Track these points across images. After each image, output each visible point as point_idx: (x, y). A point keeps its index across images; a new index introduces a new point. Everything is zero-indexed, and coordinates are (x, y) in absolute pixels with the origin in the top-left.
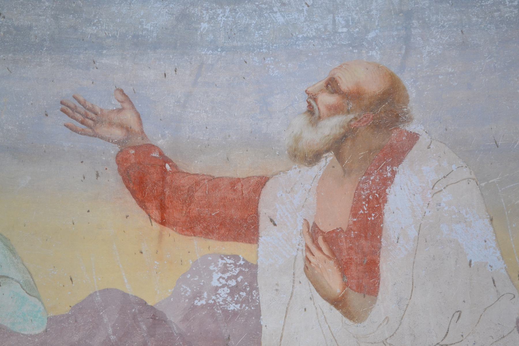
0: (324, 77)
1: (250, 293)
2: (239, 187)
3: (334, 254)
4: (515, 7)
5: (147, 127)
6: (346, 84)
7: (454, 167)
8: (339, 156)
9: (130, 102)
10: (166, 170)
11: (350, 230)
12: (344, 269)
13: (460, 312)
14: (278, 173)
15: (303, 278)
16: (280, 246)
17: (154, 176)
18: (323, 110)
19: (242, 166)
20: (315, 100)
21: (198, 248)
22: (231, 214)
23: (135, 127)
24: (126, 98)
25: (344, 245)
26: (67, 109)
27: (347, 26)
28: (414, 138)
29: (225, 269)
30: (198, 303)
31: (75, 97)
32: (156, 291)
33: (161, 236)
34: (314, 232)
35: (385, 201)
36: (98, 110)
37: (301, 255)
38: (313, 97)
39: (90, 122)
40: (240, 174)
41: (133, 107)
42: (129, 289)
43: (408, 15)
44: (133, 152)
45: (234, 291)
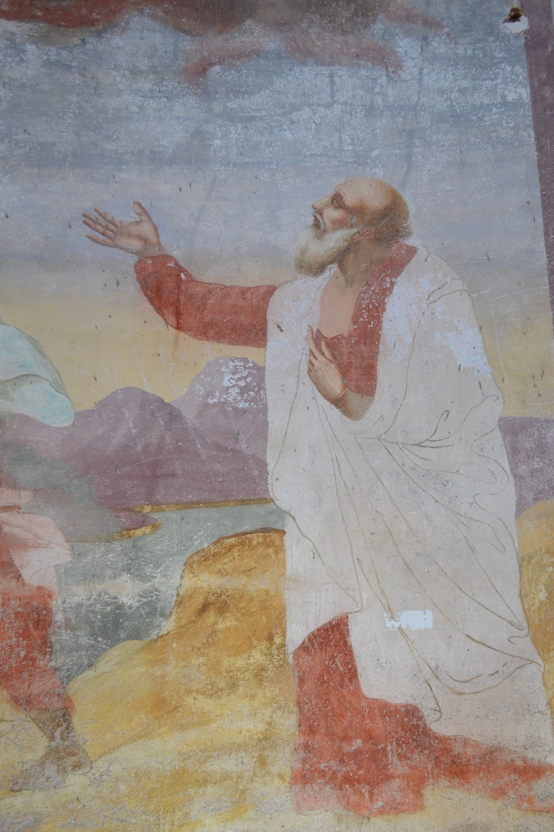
0: (330, 192)
1: (258, 393)
2: (249, 295)
4: (511, 128)
5: (164, 240)
6: (350, 200)
7: (448, 279)
8: (342, 267)
9: (148, 215)
10: (181, 279)
11: (350, 336)
12: (344, 372)
13: (448, 412)
14: (286, 283)
15: (307, 379)
16: (286, 350)
17: (170, 284)
18: (328, 224)
19: (252, 276)
20: (321, 214)
21: (211, 351)
23: (153, 239)
25: (345, 350)
26: (88, 221)
27: (353, 144)
28: (412, 251)
29: (235, 371)
30: (211, 401)
31: (96, 211)
32: (172, 390)
33: (176, 339)
34: (317, 338)
35: (384, 310)
36: (117, 222)
37: (305, 359)
39: (111, 234)
40: (250, 283)
41: (151, 220)
42: (148, 388)
43: (411, 134)
44: (150, 262)
45: (243, 390)
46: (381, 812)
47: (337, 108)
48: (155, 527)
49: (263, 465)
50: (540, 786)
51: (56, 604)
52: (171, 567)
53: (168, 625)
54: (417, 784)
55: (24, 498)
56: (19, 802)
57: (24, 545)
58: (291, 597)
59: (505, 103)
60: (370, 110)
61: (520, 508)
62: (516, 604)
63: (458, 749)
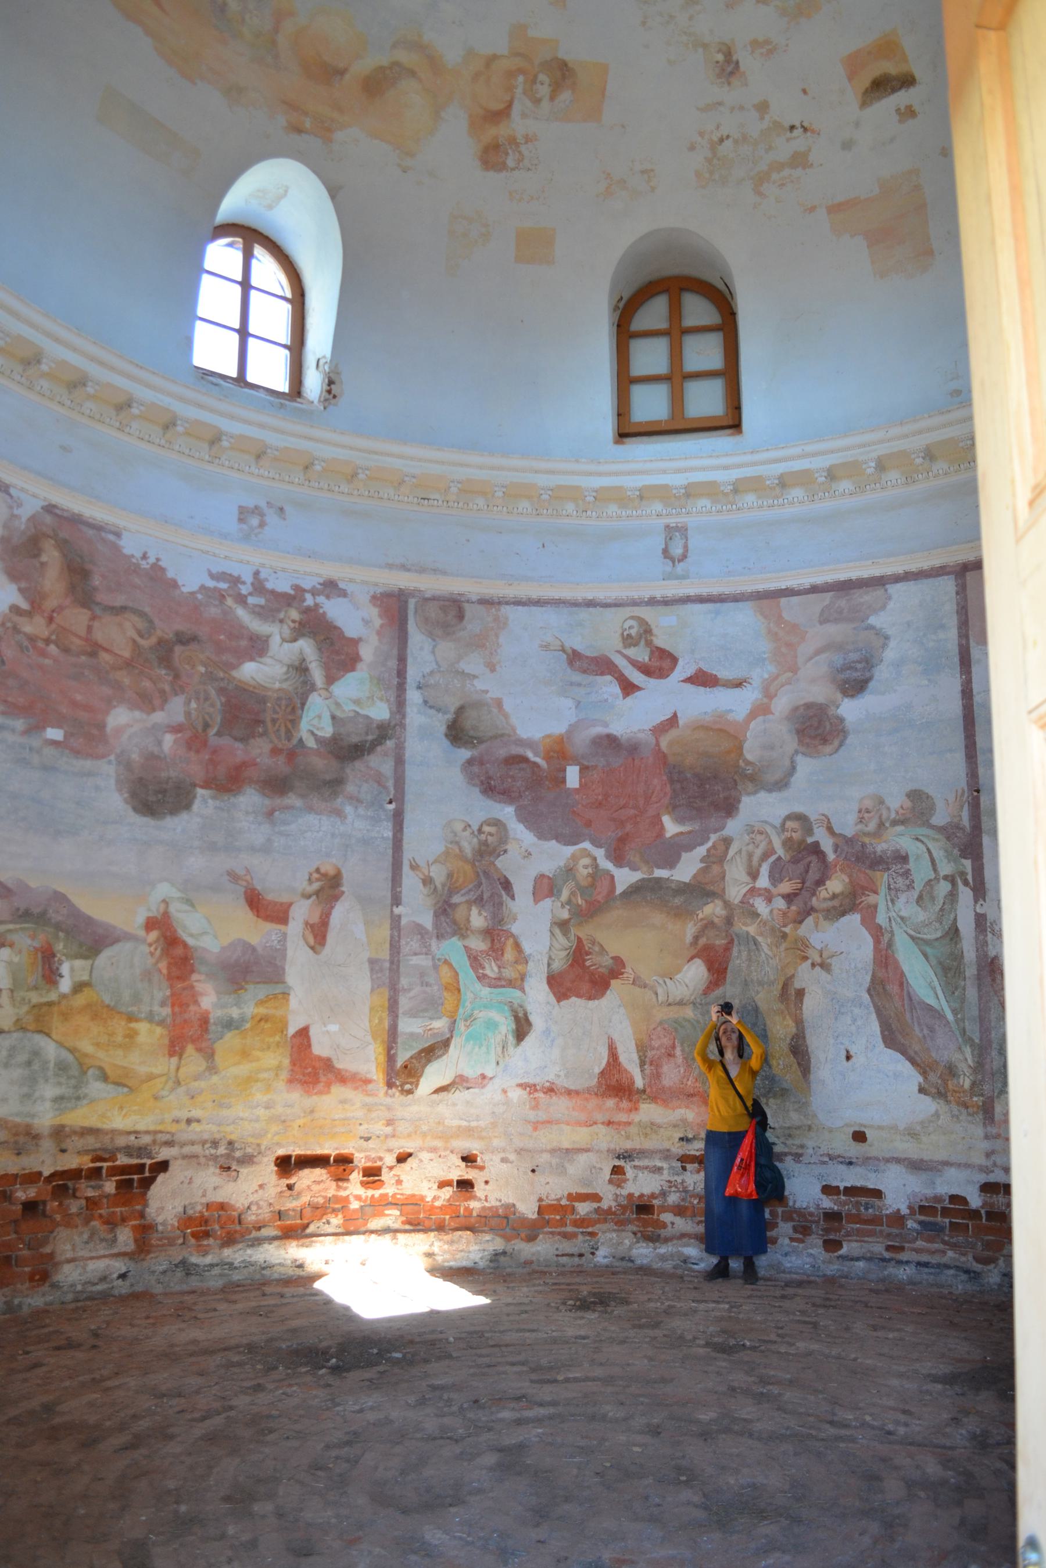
0: (315, 867)
3: (313, 931)
5: (255, 882)
6: (323, 871)
12: (315, 937)
16: (295, 927)
19: (285, 898)
21: (269, 926)
22: (279, 915)
24: (248, 871)
28: (343, 892)
32: (254, 940)
34: (307, 923)
38: (311, 874)
42: (246, 938)
46: (316, 1094)
47: (321, 833)
48: (246, 990)
49: (284, 969)
50: (370, 1086)
51: (211, 1016)
52: (249, 1005)
53: (248, 1026)
54: (328, 1085)
55: (203, 977)
56: (196, 1084)
57: (202, 994)
58: (291, 1018)
59: (383, 837)
60: (333, 835)
61: (372, 990)
62: (367, 1024)
63: (343, 1073)
